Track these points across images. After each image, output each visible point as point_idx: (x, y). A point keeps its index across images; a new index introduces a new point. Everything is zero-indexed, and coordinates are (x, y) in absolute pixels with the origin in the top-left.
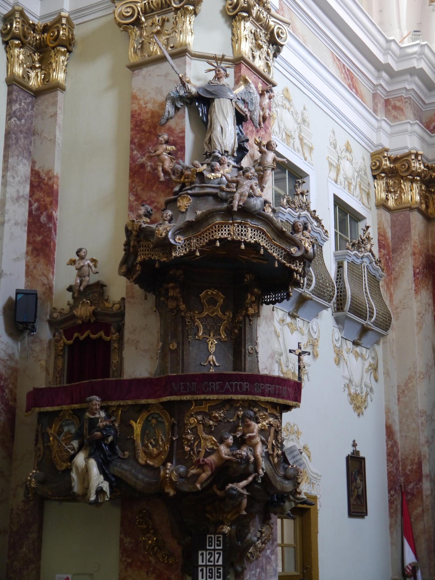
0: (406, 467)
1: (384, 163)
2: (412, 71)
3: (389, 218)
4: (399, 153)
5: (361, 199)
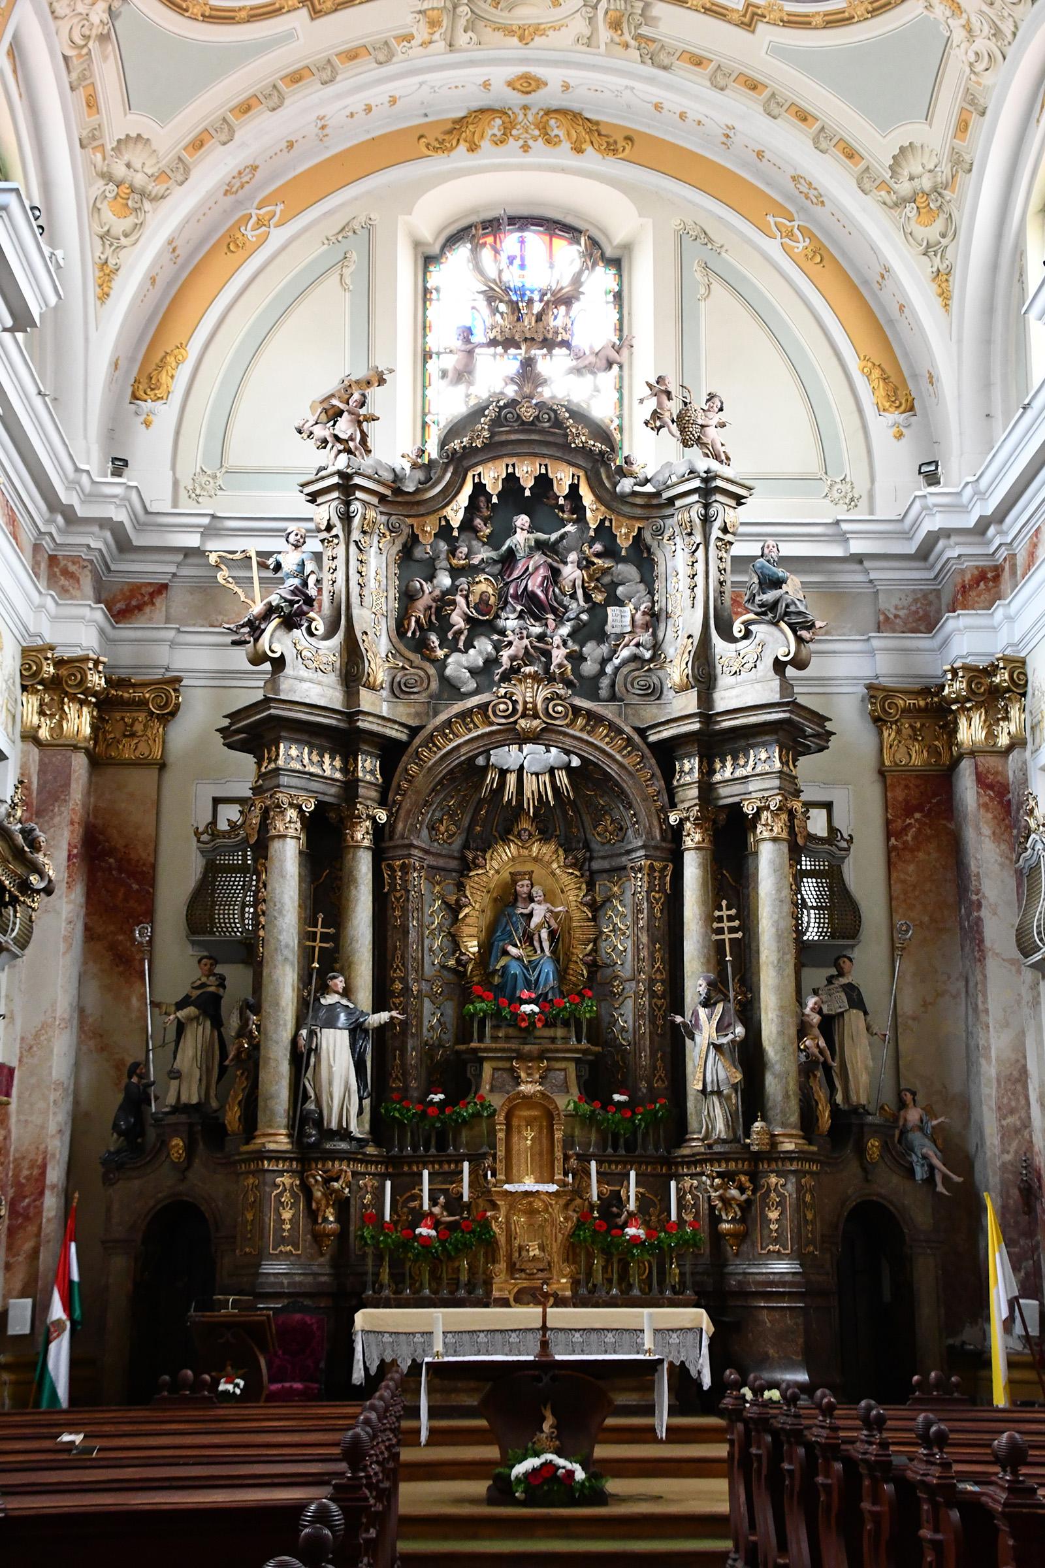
0: (21, 1171)
1: (45, 668)
2: (104, 523)
3: (37, 758)
4: (67, 654)
5: (6, 729)
